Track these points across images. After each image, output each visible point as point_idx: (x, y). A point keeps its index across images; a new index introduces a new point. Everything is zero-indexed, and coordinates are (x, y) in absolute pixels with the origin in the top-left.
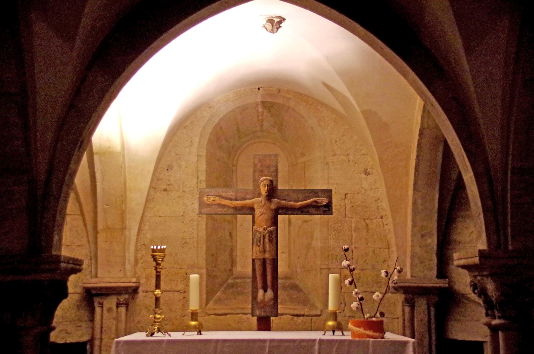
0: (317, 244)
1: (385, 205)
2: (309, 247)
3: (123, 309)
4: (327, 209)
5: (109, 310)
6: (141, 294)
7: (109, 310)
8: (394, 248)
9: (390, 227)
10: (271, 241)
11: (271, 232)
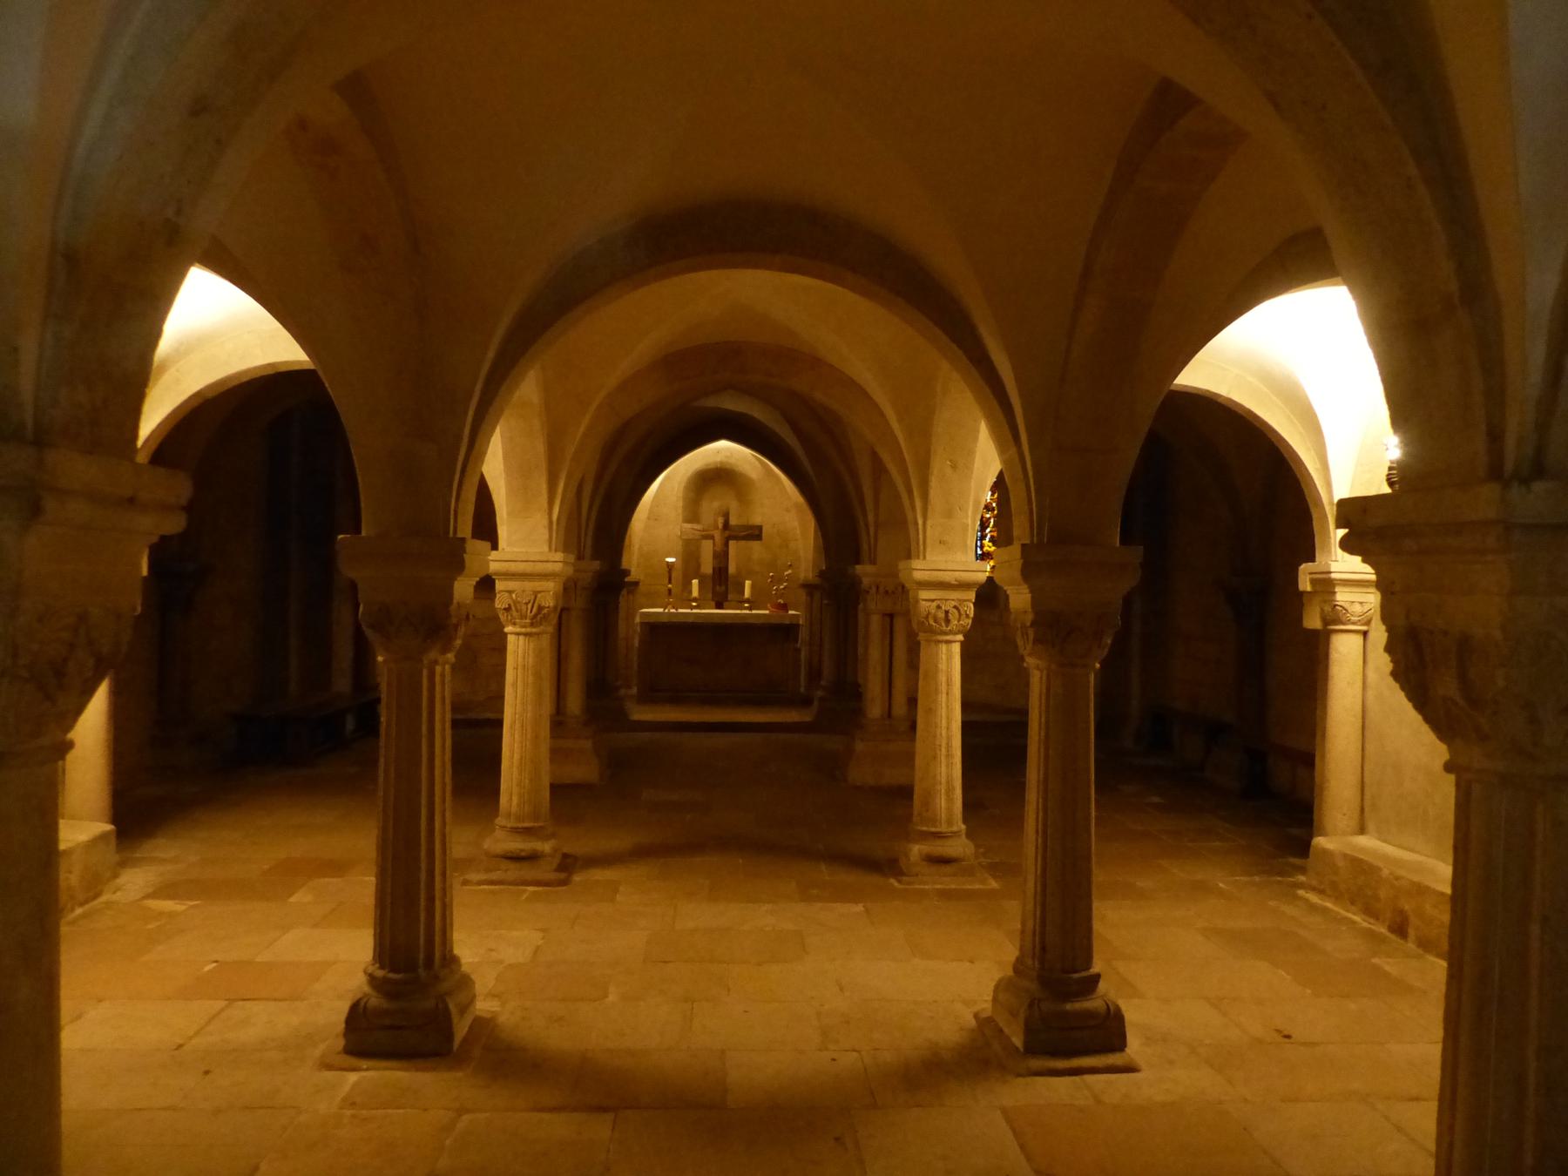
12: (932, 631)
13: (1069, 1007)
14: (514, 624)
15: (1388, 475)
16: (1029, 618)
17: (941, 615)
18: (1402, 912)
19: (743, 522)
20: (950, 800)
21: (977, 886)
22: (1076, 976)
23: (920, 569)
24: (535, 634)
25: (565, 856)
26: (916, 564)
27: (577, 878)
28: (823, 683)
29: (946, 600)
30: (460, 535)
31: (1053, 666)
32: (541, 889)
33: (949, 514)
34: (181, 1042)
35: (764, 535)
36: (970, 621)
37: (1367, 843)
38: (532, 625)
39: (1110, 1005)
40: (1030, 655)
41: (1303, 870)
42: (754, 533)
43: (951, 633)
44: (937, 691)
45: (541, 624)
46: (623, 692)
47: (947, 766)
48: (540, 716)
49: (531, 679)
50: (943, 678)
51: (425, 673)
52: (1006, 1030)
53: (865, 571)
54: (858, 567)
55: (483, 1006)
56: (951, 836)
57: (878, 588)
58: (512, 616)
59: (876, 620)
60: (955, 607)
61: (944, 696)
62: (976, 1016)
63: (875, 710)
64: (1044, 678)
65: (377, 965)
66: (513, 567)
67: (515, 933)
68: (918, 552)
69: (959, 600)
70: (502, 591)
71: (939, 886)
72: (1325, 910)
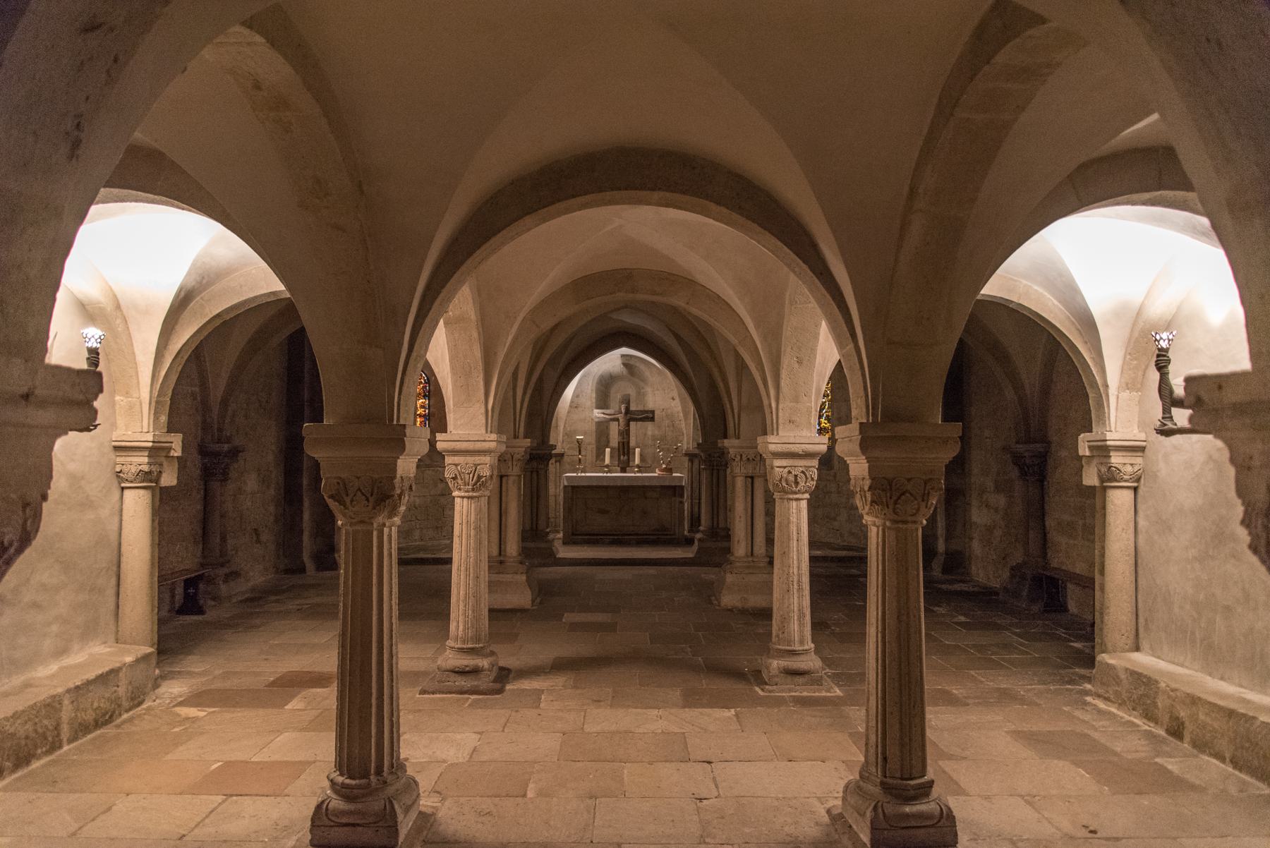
0: (650, 433)
1: (681, 415)
2: (645, 434)
3: (558, 464)
4: (652, 419)
5: (552, 464)
6: (565, 457)
7: (552, 464)
8: (685, 435)
9: (684, 425)
10: (626, 434)
11: (626, 430)
12: (784, 491)
13: (907, 809)
14: (460, 489)
15: (1156, 361)
16: (868, 483)
17: (791, 478)
18: (1177, 718)
19: (640, 408)
20: (801, 625)
21: (824, 694)
22: (912, 782)
23: (773, 443)
24: (476, 497)
25: (502, 669)
26: (771, 439)
27: (508, 687)
28: (701, 528)
29: (795, 467)
30: (402, 422)
31: (888, 524)
32: (481, 697)
33: (796, 399)
34: (184, 833)
35: (656, 417)
36: (815, 483)
37: (1144, 660)
38: (473, 490)
39: (943, 807)
40: (867, 514)
41: (1089, 679)
42: (649, 416)
43: (799, 492)
44: (789, 539)
45: (481, 490)
46: (551, 536)
47: (799, 598)
48: (480, 560)
49: (473, 533)
50: (793, 528)
51: (375, 533)
52: (854, 827)
53: (730, 444)
54: (725, 441)
55: (427, 803)
56: (803, 654)
57: (741, 455)
58: (458, 483)
59: (740, 482)
60: (803, 472)
61: (795, 542)
62: (828, 811)
63: (740, 550)
64: (880, 533)
65: (338, 773)
66: (459, 446)
67: (458, 736)
68: (773, 430)
69: (805, 466)
70: (450, 464)
71: (793, 694)
72: (1110, 713)
